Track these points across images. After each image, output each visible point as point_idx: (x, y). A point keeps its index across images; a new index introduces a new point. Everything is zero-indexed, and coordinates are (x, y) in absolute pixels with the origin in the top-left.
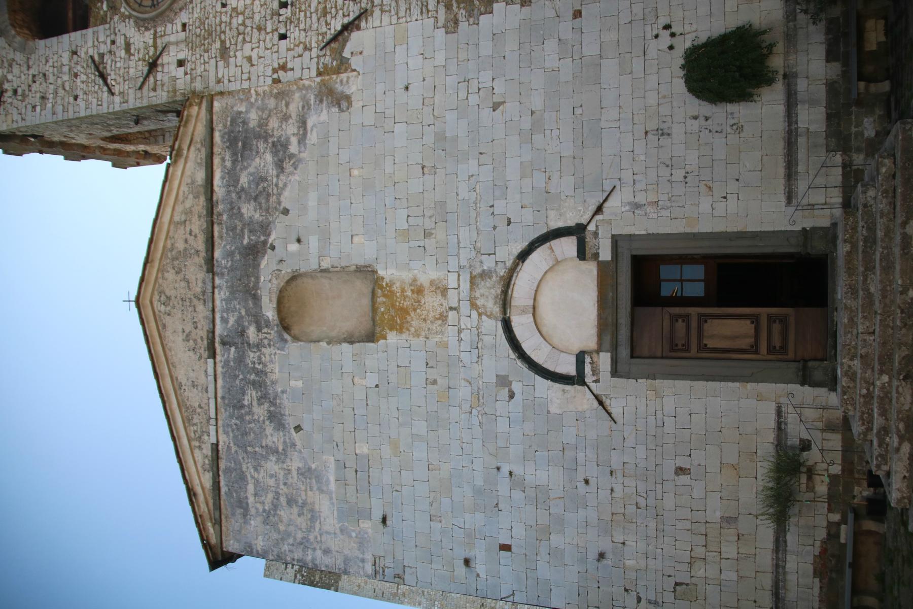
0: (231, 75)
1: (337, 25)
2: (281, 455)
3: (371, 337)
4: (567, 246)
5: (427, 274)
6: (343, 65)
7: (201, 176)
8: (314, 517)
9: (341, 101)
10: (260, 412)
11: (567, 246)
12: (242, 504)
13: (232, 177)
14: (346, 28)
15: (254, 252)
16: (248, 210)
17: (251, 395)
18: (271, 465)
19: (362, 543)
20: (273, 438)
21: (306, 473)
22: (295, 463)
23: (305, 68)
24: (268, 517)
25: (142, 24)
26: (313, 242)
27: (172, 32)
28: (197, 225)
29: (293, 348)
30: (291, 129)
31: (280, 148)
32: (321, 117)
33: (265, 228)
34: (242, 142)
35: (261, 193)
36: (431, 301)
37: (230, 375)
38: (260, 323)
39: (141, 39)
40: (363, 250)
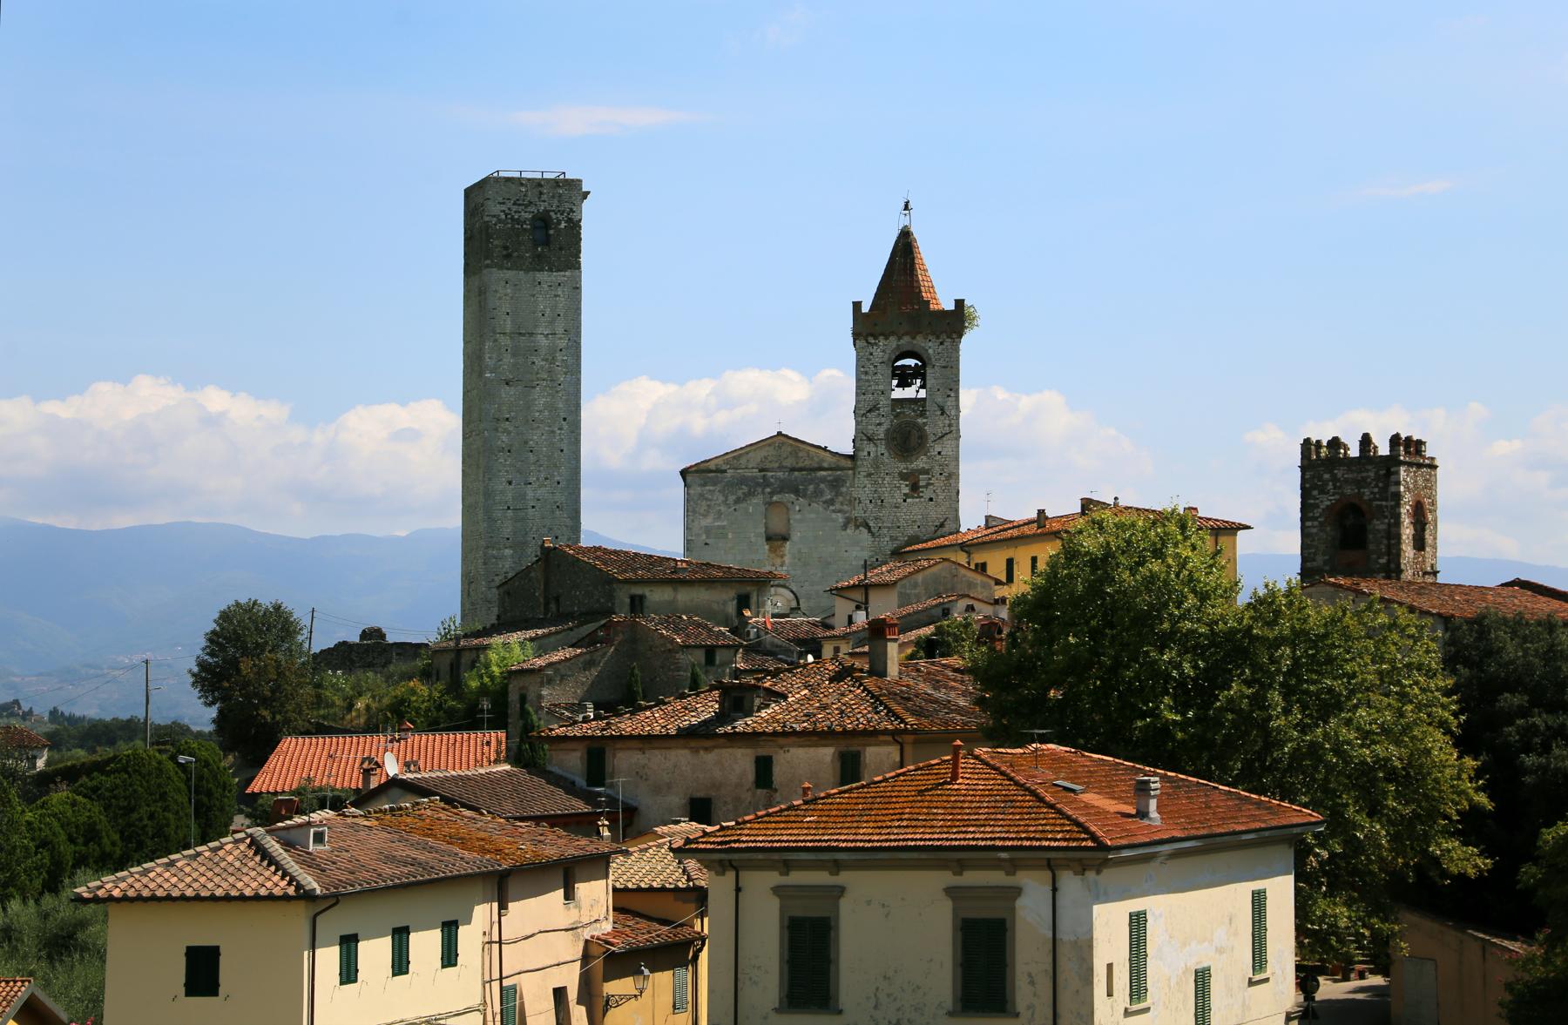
0: (861, 479)
1: (871, 524)
2: (725, 502)
3: (769, 539)
4: (794, 604)
5: (787, 559)
6: (857, 527)
7: (825, 465)
8: (705, 516)
9: (845, 527)
10: (740, 493)
11: (794, 604)
12: (705, 485)
13: (823, 480)
14: (869, 528)
15: (797, 492)
16: (811, 487)
17: (745, 489)
18: (721, 498)
19: (698, 535)
20: (732, 498)
21: (720, 513)
22: (723, 508)
23: (858, 512)
24: (701, 495)
25: (887, 431)
26: (798, 516)
27: (882, 449)
28: (807, 463)
29: (763, 508)
30: (838, 506)
31: (831, 502)
32: (840, 518)
33: (804, 496)
34: (836, 484)
35: (818, 493)
36: (778, 561)
37: (753, 479)
38: (772, 494)
39: (881, 432)
40: (796, 536)
